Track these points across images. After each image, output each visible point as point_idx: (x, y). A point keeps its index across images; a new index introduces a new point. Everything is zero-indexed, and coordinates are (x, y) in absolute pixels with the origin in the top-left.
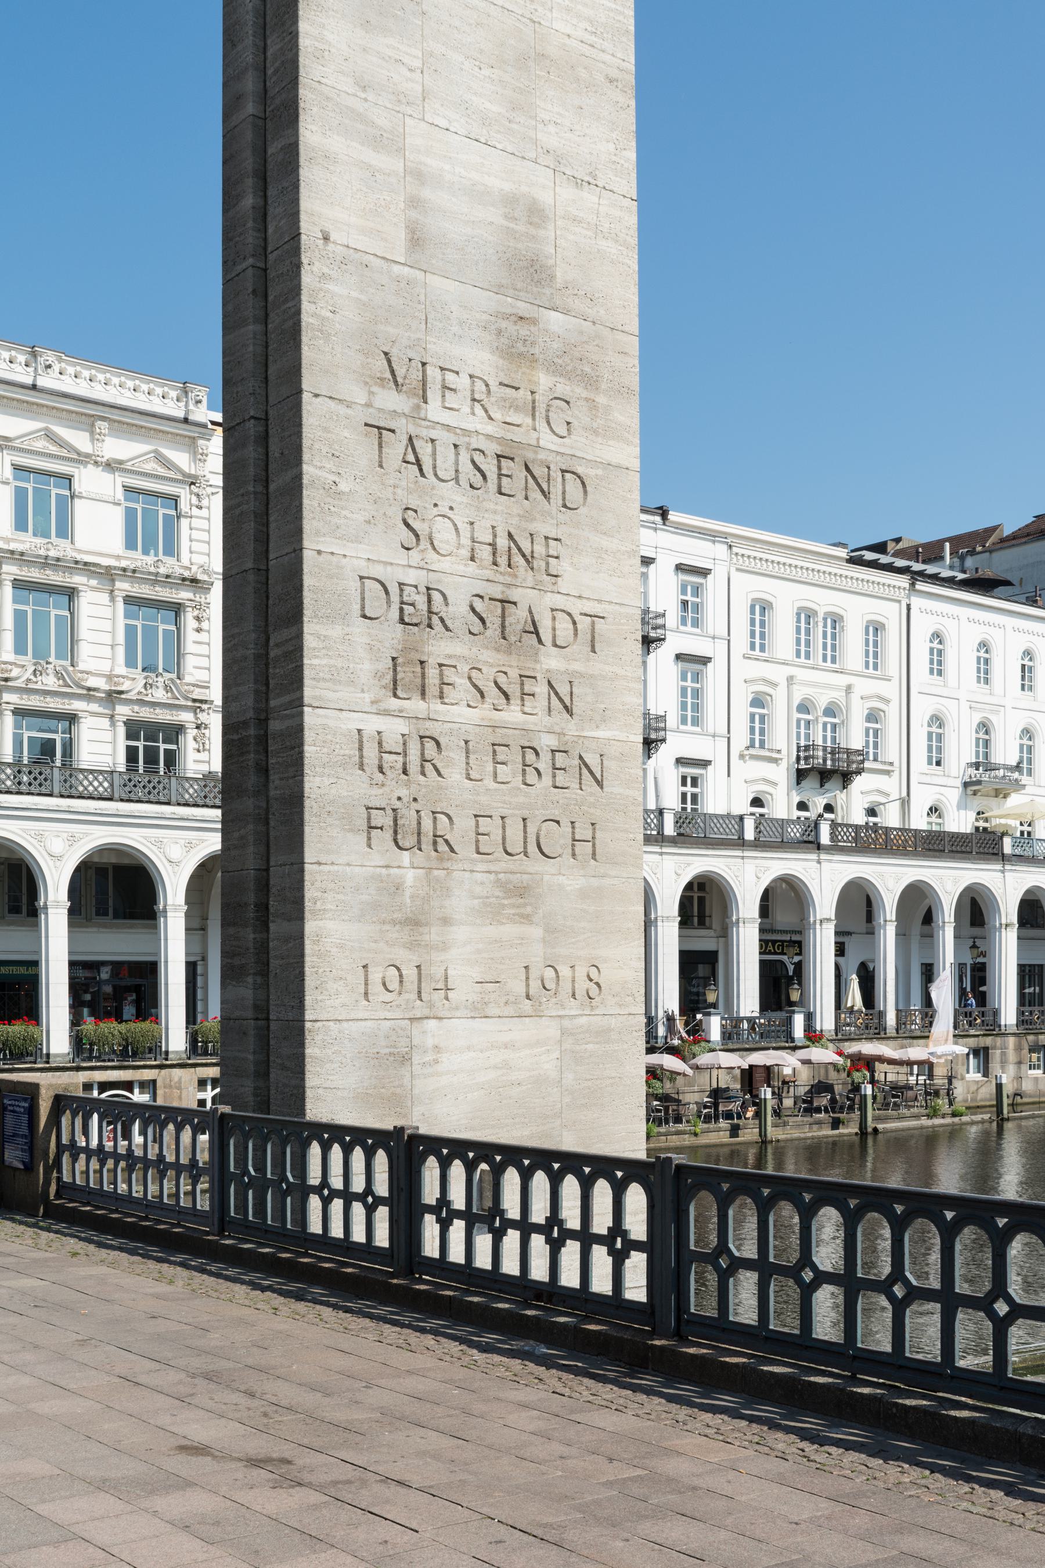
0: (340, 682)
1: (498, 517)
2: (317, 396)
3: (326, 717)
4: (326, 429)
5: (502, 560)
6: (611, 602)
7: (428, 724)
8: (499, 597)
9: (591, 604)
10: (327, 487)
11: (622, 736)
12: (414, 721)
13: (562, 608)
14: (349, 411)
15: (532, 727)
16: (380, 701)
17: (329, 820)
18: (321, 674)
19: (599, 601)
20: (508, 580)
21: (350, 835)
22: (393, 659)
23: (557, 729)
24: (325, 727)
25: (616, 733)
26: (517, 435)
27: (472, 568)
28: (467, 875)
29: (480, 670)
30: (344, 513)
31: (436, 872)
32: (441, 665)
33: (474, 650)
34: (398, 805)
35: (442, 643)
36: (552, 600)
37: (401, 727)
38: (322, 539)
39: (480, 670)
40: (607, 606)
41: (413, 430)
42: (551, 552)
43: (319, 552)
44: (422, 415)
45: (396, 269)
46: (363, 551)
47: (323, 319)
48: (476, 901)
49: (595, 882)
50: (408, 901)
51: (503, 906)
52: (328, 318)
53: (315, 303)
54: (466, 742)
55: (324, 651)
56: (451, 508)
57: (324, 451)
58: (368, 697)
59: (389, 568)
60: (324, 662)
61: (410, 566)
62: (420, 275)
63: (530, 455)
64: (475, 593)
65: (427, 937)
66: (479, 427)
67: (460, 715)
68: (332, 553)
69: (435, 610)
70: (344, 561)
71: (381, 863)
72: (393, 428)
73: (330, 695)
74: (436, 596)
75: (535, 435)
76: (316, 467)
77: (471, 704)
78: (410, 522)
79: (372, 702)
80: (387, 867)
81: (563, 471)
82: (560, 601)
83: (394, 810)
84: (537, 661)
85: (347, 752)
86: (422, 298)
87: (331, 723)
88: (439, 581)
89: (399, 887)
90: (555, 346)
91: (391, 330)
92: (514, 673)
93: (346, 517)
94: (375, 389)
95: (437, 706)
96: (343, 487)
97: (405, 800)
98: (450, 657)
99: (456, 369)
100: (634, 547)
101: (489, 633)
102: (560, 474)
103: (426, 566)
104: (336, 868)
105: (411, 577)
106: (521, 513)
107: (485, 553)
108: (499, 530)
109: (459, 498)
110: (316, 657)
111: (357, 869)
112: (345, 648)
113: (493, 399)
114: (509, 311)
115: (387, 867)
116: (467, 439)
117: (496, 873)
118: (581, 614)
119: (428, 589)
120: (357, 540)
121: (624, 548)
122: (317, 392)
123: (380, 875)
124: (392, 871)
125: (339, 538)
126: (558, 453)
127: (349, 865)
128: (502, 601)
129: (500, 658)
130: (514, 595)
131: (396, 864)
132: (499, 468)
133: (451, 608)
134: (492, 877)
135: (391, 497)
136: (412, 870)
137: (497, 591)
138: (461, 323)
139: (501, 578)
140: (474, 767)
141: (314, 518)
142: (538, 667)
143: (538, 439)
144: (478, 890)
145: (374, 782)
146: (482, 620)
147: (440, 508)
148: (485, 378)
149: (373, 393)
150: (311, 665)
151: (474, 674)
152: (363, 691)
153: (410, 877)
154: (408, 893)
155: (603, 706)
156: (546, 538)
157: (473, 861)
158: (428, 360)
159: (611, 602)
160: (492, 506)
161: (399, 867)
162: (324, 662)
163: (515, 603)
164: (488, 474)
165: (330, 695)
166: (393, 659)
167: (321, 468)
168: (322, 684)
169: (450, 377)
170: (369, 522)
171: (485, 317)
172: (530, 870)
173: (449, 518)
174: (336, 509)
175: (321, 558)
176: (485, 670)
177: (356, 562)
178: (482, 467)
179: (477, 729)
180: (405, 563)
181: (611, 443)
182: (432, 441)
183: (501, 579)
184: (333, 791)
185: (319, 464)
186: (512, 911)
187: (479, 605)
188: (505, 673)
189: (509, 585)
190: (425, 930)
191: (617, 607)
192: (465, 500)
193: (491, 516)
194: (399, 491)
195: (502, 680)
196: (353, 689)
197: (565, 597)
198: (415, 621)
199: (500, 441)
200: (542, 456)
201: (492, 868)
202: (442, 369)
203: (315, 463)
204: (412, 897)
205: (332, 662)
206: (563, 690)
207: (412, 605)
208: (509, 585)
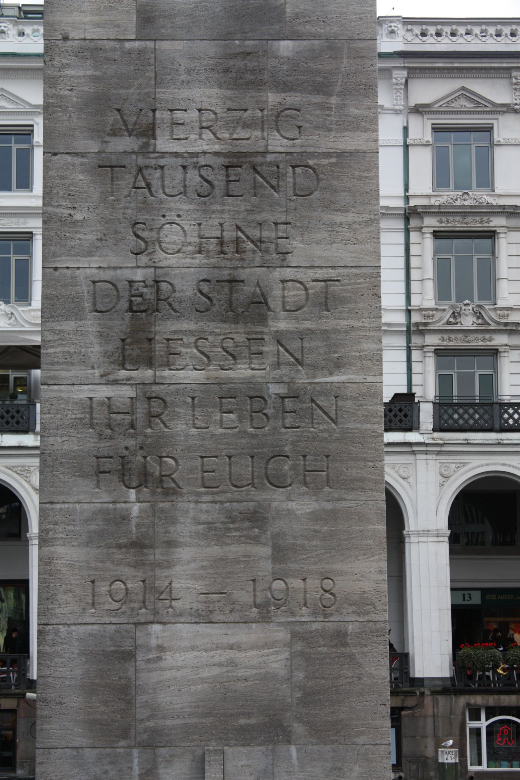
0: (72, 364)
1: (226, 216)
2: (55, 154)
3: (60, 391)
4: (63, 178)
5: (230, 249)
6: (345, 267)
7: (154, 388)
8: (227, 278)
9: (324, 271)
10: (63, 219)
11: (359, 378)
12: (141, 386)
13: (292, 278)
14: (84, 160)
15: (259, 380)
16: (109, 374)
17: (62, 469)
18: (56, 359)
19: (333, 267)
20: (236, 263)
21: (80, 480)
22: (123, 340)
23: (286, 379)
24: (58, 398)
25: (352, 376)
26: (245, 147)
27: (199, 259)
28: (192, 505)
29: (206, 339)
30: (78, 236)
31: (161, 505)
32: (168, 340)
33: (201, 324)
34: (126, 453)
35: (169, 323)
36: (278, 274)
37: (128, 392)
38: (59, 259)
39: (206, 339)
40: (342, 271)
41: (141, 161)
42: (280, 234)
43: (56, 269)
44: (151, 150)
45: (128, 45)
46: (95, 261)
47: (62, 97)
48: (201, 527)
49: (328, 506)
50: (134, 529)
51: (229, 530)
52: (66, 96)
53: (55, 87)
54: (193, 398)
55: (59, 342)
56: (179, 216)
57: (61, 193)
58: (97, 372)
59: (119, 272)
60: (59, 349)
61: (138, 267)
62: (150, 44)
63: (259, 159)
64: (201, 278)
65: (152, 557)
66: (206, 148)
67: (185, 378)
68: (68, 268)
69: (162, 297)
70: (78, 272)
71: (108, 500)
72: (123, 164)
73: (64, 374)
74: (164, 286)
75: (263, 143)
76: (54, 206)
77: (197, 367)
78: (139, 233)
79: (102, 376)
80: (114, 502)
81: (294, 167)
82: (289, 273)
83: (123, 457)
84: (267, 326)
85: (78, 416)
86: (152, 61)
87: (64, 395)
88: (166, 275)
89: (125, 518)
90: (285, 67)
91: (122, 91)
92: (241, 338)
93: (80, 239)
94: (107, 139)
95: (167, 373)
96: (78, 216)
97: (132, 449)
98: (176, 332)
99: (184, 108)
100: (372, 217)
101: (214, 309)
102: (290, 170)
103: (153, 265)
104: (67, 506)
105: (139, 275)
106: (249, 208)
107: (213, 245)
108: (226, 226)
109: (185, 207)
110: (52, 347)
111: (86, 506)
112: (77, 337)
113: (219, 123)
114: (238, 50)
115: (114, 502)
116: (195, 160)
117: (222, 503)
118: (313, 281)
119: (156, 282)
120: (90, 254)
121: (361, 219)
122: (56, 151)
123: (107, 509)
124: (118, 506)
125: (74, 255)
126: (287, 153)
127: (79, 503)
128: (230, 281)
129: (226, 327)
130: (243, 274)
131: (123, 500)
132: (227, 176)
133: (177, 295)
134: (217, 506)
135: (121, 216)
136: (138, 504)
137: (225, 274)
138: (189, 72)
139: (228, 264)
140: (199, 418)
141: (51, 244)
142: (266, 330)
143: (266, 146)
144: (203, 517)
145: (103, 437)
146: (209, 298)
147: (167, 218)
148: (212, 108)
149: (106, 142)
150: (47, 354)
151: (200, 343)
152: (93, 368)
153: (135, 509)
154: (134, 522)
155: (336, 355)
156: (276, 224)
157: (200, 494)
158: (158, 106)
159: (345, 267)
160: (219, 207)
161: (126, 502)
162: (59, 349)
163: (242, 281)
164: (215, 183)
165: (64, 374)
166: (123, 340)
167: (58, 206)
168: (57, 367)
169: (178, 115)
170: (101, 239)
171: (212, 61)
172: (257, 498)
173: (177, 224)
174: (71, 235)
175: (57, 273)
176: (211, 338)
177: (88, 271)
178: (209, 178)
179: (203, 387)
180: (135, 265)
181: (344, 134)
182: (162, 167)
183: (228, 264)
184: (65, 447)
185: (56, 204)
186: (237, 533)
187: (205, 288)
188: (232, 339)
189: (236, 268)
190: (151, 551)
191: (353, 270)
192: (192, 207)
193: (218, 215)
194: (129, 212)
195: (229, 344)
196: (84, 368)
197: (296, 270)
198: (143, 308)
199: (225, 155)
200: (270, 158)
201: (217, 498)
202: (171, 110)
203: (53, 203)
204: (137, 526)
205: (65, 349)
206: (294, 346)
207: (141, 295)
208: (236, 268)
